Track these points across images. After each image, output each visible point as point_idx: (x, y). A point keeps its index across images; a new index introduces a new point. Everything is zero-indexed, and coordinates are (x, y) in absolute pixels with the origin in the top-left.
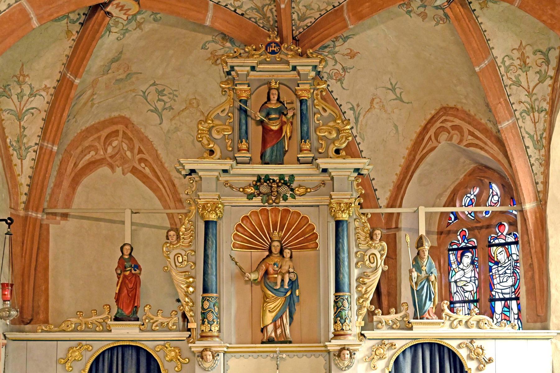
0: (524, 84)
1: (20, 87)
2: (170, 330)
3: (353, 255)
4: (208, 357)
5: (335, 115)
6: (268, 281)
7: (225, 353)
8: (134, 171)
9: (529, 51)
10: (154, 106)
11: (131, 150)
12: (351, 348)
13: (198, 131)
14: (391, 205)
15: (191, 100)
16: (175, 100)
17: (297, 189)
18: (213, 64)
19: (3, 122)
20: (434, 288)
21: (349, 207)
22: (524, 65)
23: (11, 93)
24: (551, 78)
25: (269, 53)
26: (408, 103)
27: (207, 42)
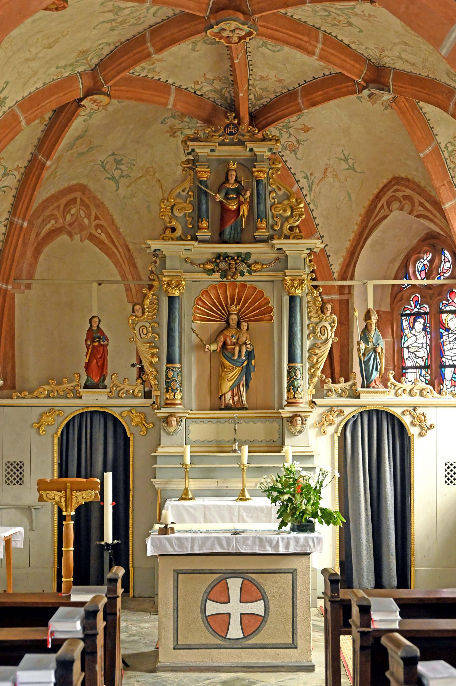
2: (136, 397)
3: (305, 327)
4: (173, 422)
5: (289, 194)
6: (225, 352)
7: (187, 418)
8: (92, 238)
10: (112, 174)
11: (88, 216)
12: (302, 415)
13: (160, 209)
14: (343, 278)
15: (148, 168)
16: (132, 169)
17: (253, 265)
18: (170, 136)
20: (381, 359)
21: (302, 283)
25: (228, 134)
26: (360, 173)
27: (166, 118)
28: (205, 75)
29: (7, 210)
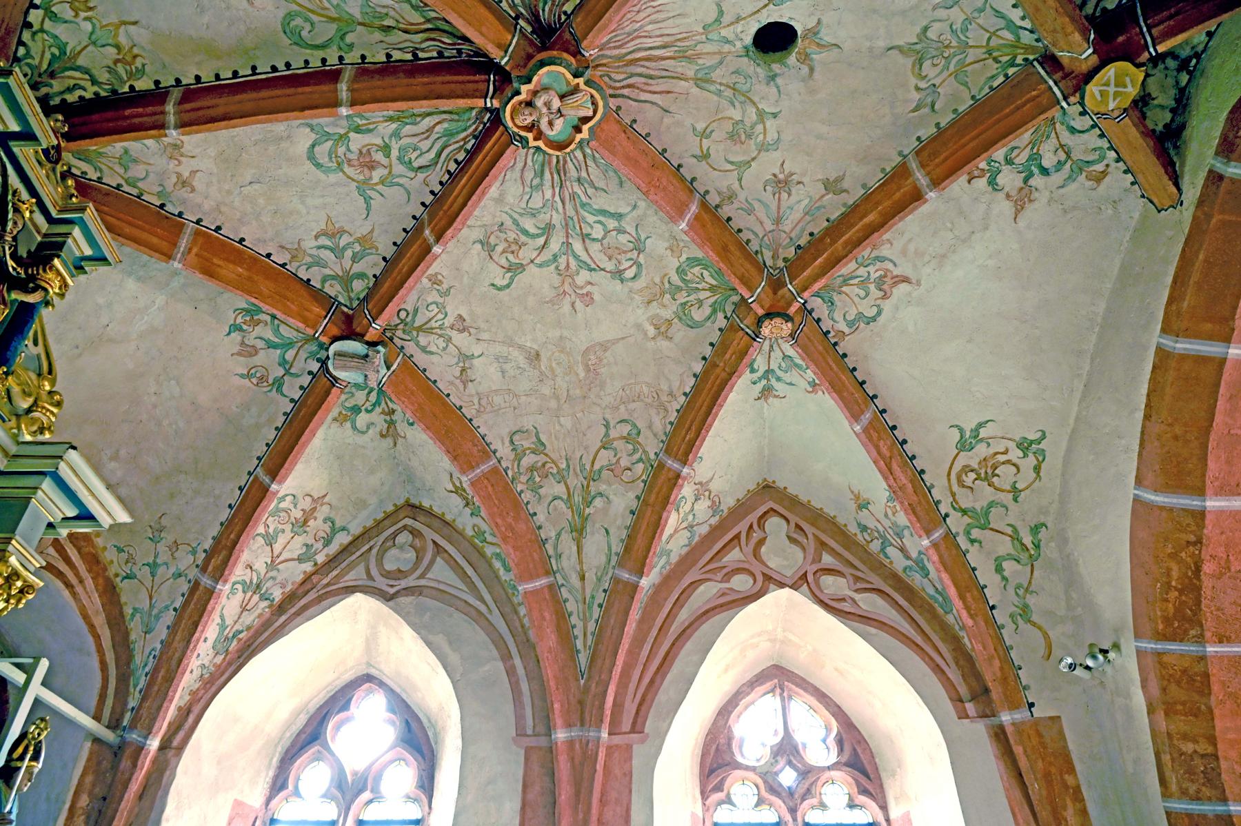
0: (278, 547)
9: (323, 512)
22: (301, 525)
24: (316, 564)
28: (135, 23)
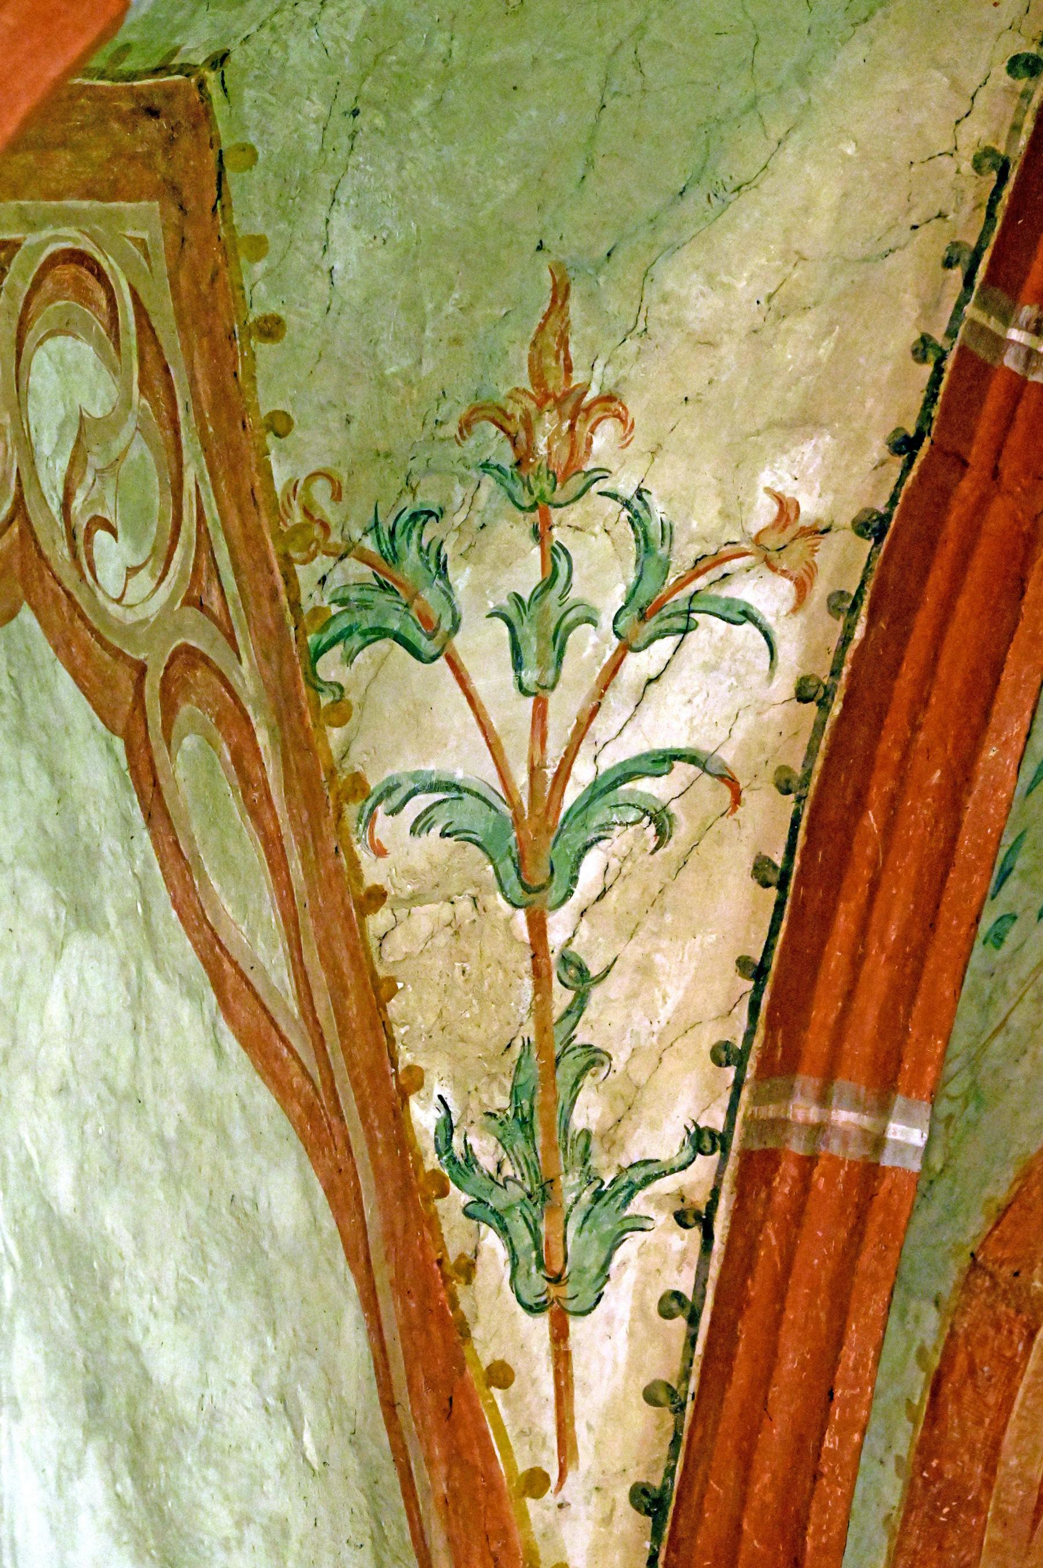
1: (539, 535)
19: (378, 921)
23: (448, 592)
29: (710, 1036)
